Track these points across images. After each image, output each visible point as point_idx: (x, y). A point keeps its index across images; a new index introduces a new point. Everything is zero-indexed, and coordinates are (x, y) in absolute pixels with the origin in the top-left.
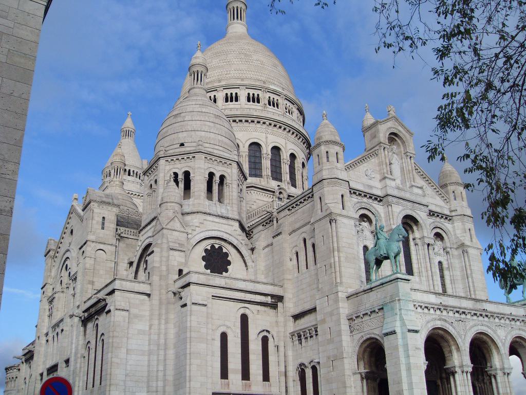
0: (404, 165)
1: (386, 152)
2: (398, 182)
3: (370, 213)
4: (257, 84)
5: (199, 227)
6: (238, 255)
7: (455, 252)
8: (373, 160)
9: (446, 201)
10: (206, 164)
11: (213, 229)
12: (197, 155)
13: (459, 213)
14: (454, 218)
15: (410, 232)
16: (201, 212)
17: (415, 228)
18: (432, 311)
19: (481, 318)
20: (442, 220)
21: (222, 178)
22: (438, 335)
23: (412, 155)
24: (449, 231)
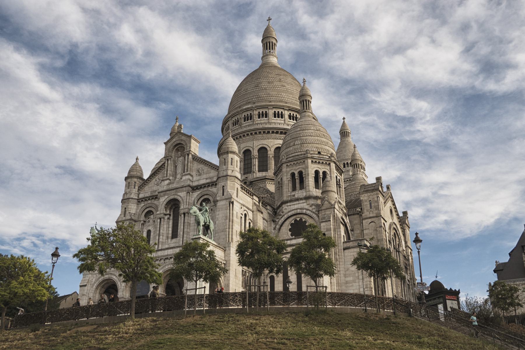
23: (187, 153)
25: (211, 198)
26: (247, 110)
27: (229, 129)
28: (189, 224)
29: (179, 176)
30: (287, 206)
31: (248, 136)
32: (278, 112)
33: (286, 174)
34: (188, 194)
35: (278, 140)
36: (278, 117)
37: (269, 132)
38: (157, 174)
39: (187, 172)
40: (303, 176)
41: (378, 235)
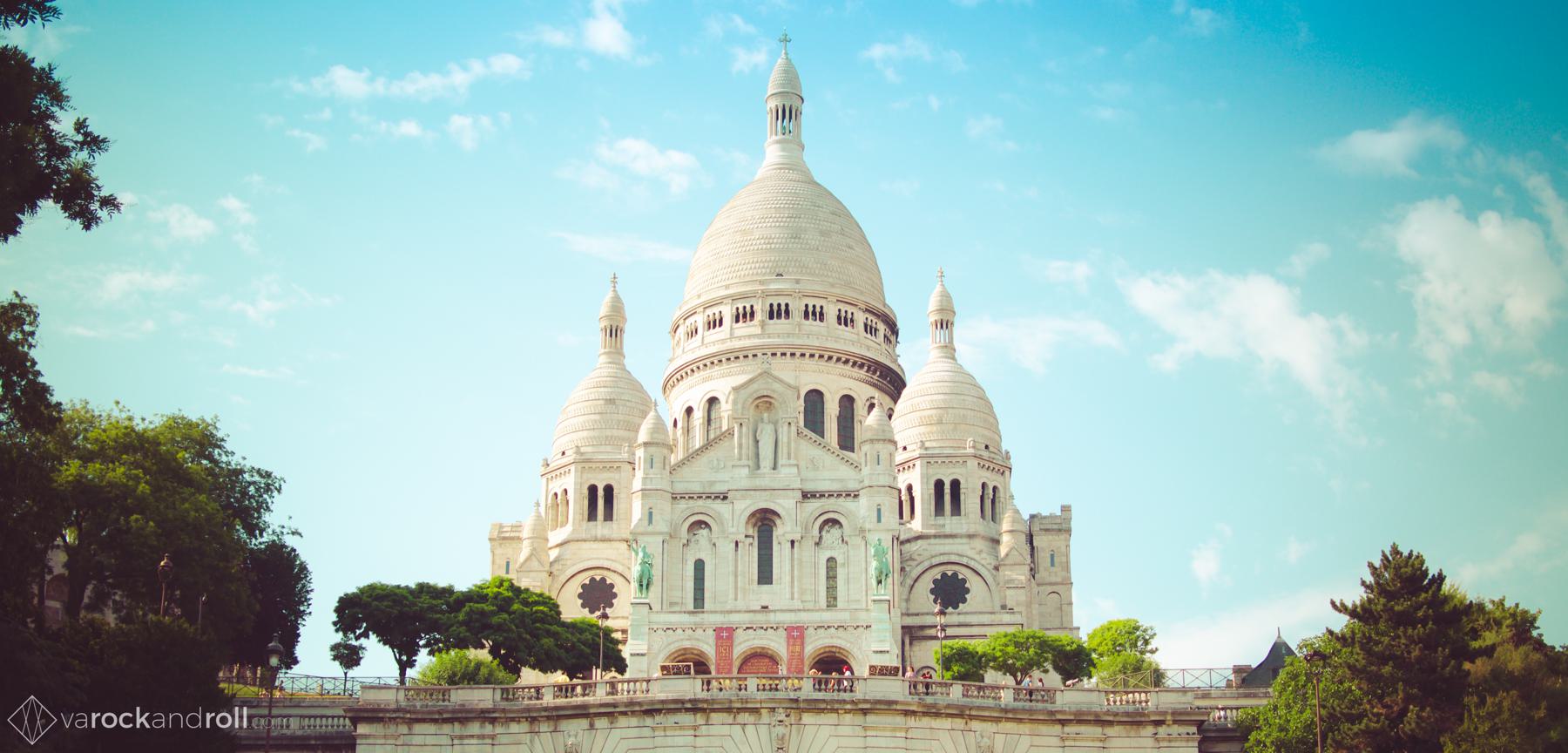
0: (780, 437)
2: (766, 462)
3: (710, 518)
6: (627, 583)
7: (859, 540)
8: (727, 444)
10: (585, 476)
13: (867, 483)
15: (774, 529)
16: (572, 541)
17: (778, 522)
18: (679, 631)
20: (841, 500)
21: (609, 490)
22: (693, 654)
23: (790, 420)
25: (842, 520)
26: (778, 294)
27: (721, 324)
28: (800, 561)
29: (766, 462)
31: (784, 357)
32: (846, 312)
33: (925, 480)
34: (798, 504)
35: (846, 379)
36: (846, 325)
37: (830, 358)
38: (712, 448)
39: (789, 458)
40: (962, 491)
41: (1064, 619)
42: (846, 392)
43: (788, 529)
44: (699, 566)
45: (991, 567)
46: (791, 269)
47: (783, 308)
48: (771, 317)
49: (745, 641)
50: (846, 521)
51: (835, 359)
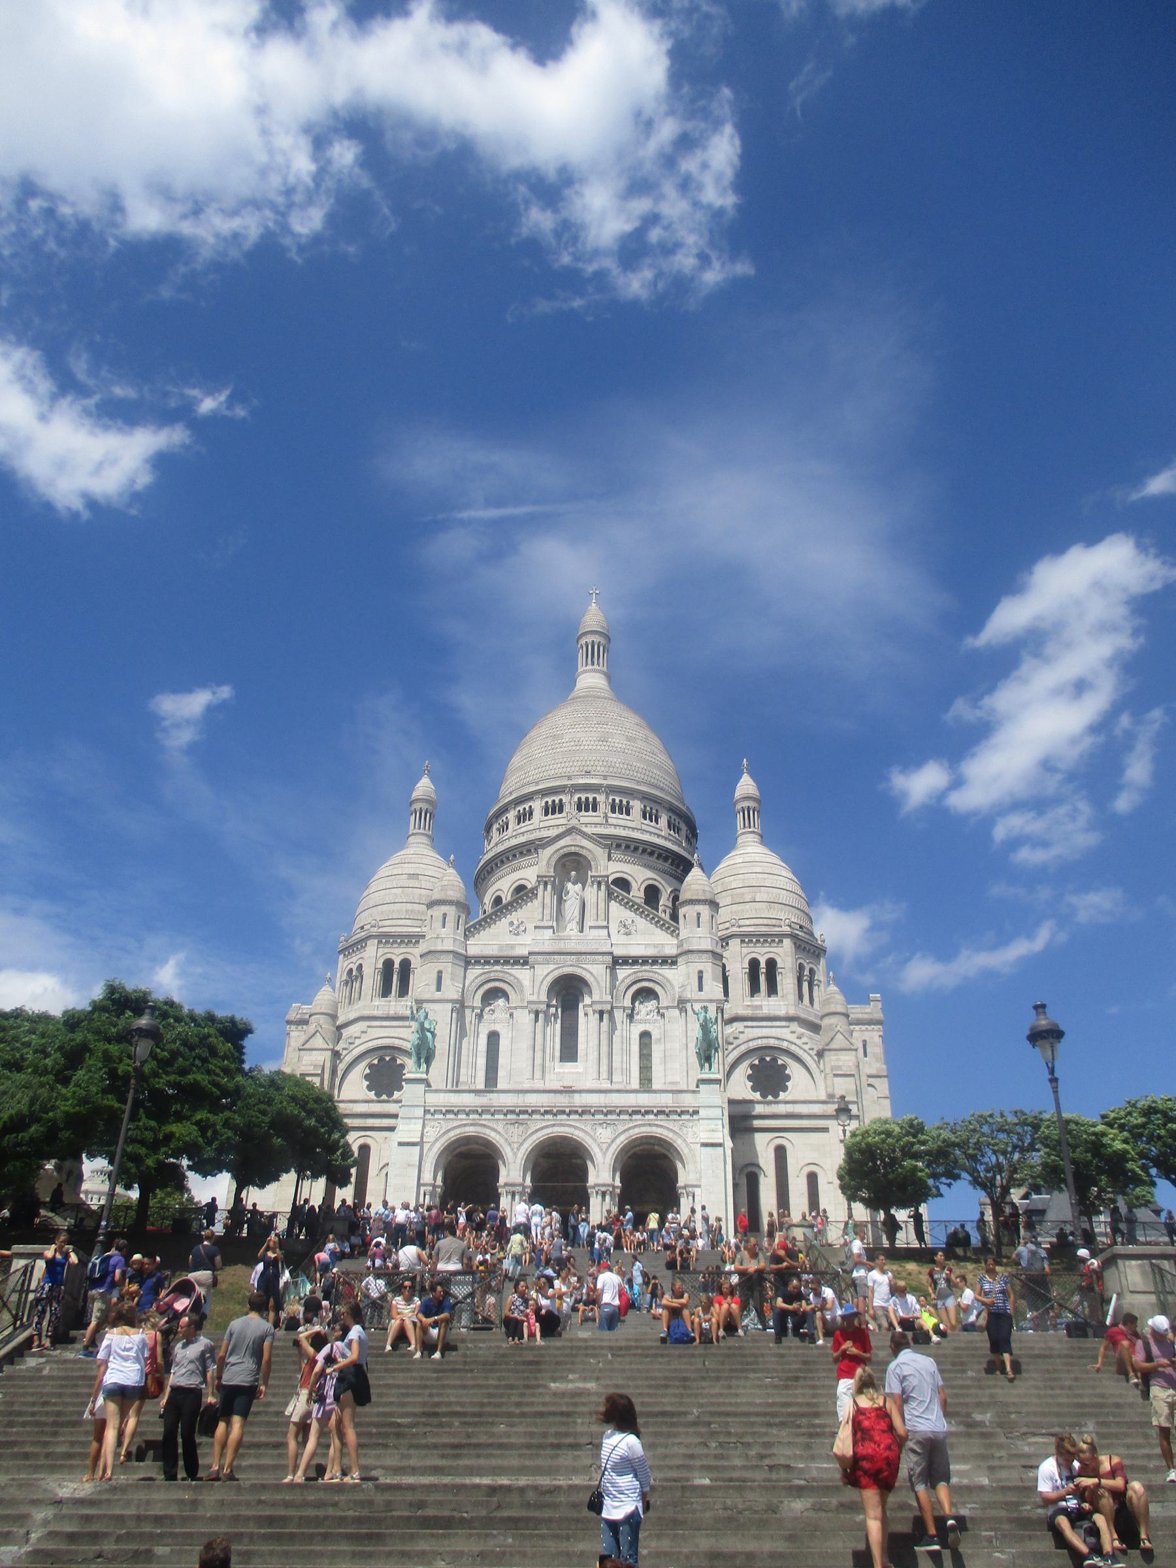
1: (549, 887)
4: (558, 783)
5: (359, 1038)
7: (677, 1012)
9: (674, 932)
10: (381, 951)
11: (382, 1035)
12: (369, 942)
13: (686, 947)
14: (679, 960)
15: (581, 998)
17: (585, 990)
19: (559, 1117)
21: (406, 965)
22: (477, 1144)
24: (668, 980)
25: (658, 989)
30: (745, 1027)
32: (651, 808)
37: (636, 849)
42: (651, 882)
43: (596, 997)
44: (494, 1037)
45: (813, 1053)
46: (598, 768)
47: (591, 800)
48: (580, 809)
49: (542, 1128)
50: (663, 992)
51: (641, 849)
